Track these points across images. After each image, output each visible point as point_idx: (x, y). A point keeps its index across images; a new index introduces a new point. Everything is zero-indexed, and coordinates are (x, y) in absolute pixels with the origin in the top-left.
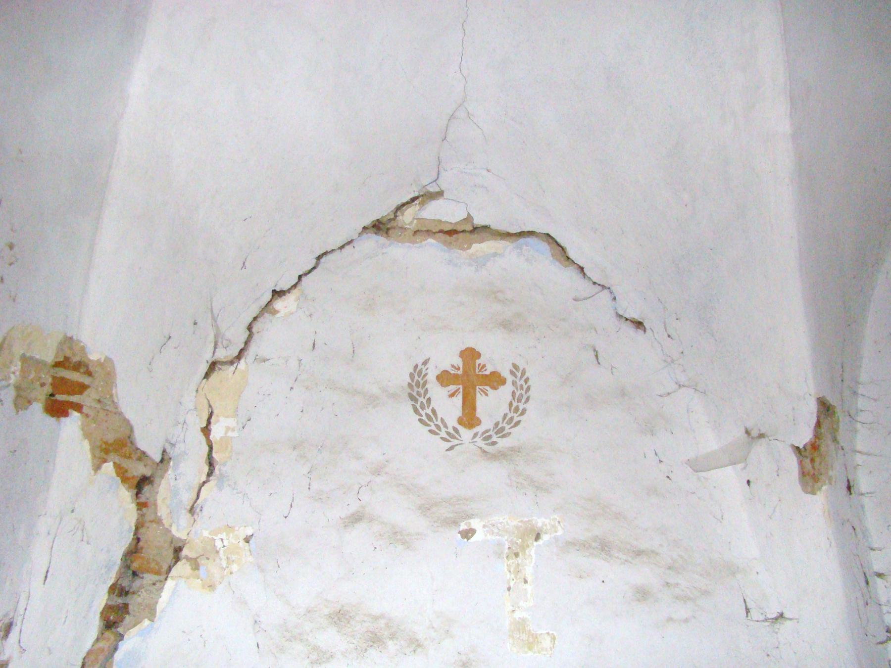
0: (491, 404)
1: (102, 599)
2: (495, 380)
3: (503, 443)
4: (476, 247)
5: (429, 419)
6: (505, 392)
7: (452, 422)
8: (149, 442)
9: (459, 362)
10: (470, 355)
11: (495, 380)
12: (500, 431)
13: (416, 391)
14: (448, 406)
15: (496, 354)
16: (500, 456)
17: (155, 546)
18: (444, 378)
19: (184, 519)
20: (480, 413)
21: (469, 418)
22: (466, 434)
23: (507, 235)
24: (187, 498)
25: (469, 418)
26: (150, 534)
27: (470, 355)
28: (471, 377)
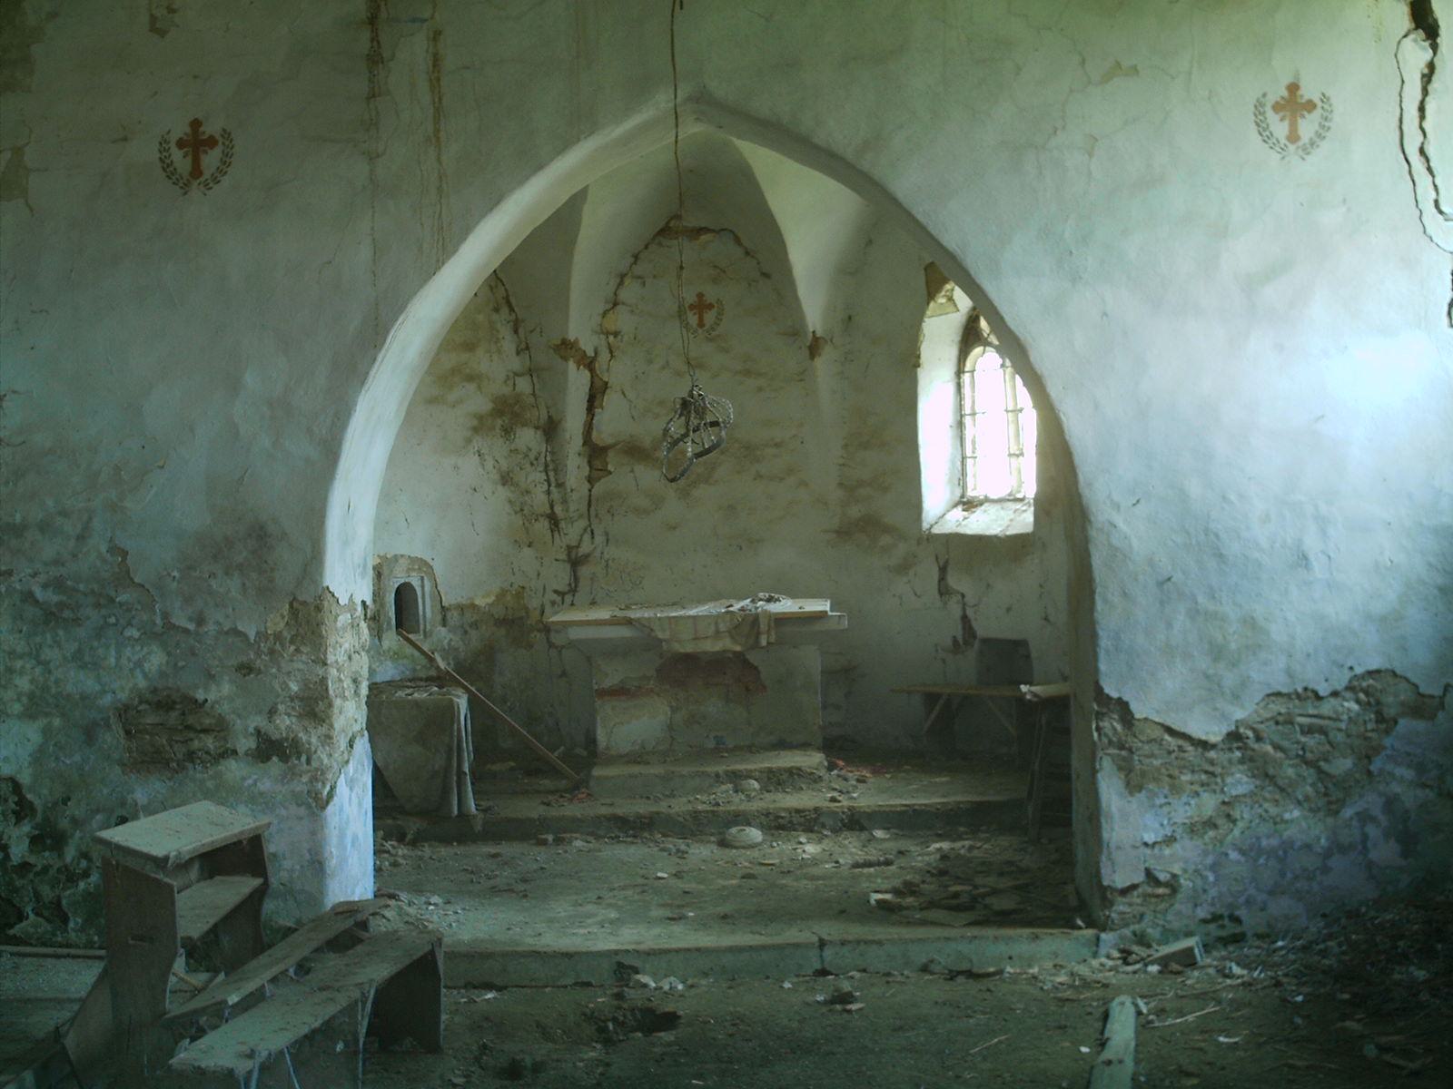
0: (710, 317)
1: (585, 406)
2: (710, 306)
3: (713, 333)
4: (703, 237)
5: (687, 326)
6: (714, 311)
7: (695, 326)
8: (590, 353)
9: (696, 299)
10: (700, 296)
11: (710, 306)
12: (713, 329)
13: (681, 314)
14: (693, 319)
15: (711, 294)
16: (711, 340)
17: (598, 384)
18: (692, 307)
19: (606, 374)
20: (705, 322)
21: (701, 324)
22: (700, 331)
23: (713, 231)
24: (605, 367)
25: (701, 324)
26: (596, 380)
27: (700, 296)
28: (701, 306)
